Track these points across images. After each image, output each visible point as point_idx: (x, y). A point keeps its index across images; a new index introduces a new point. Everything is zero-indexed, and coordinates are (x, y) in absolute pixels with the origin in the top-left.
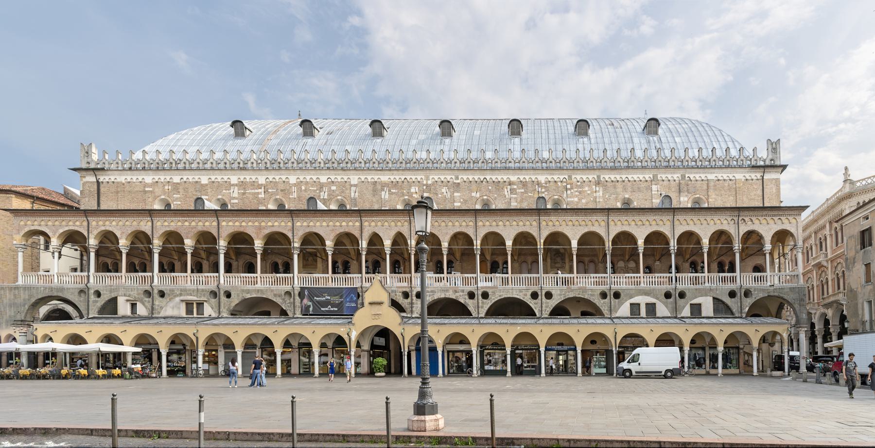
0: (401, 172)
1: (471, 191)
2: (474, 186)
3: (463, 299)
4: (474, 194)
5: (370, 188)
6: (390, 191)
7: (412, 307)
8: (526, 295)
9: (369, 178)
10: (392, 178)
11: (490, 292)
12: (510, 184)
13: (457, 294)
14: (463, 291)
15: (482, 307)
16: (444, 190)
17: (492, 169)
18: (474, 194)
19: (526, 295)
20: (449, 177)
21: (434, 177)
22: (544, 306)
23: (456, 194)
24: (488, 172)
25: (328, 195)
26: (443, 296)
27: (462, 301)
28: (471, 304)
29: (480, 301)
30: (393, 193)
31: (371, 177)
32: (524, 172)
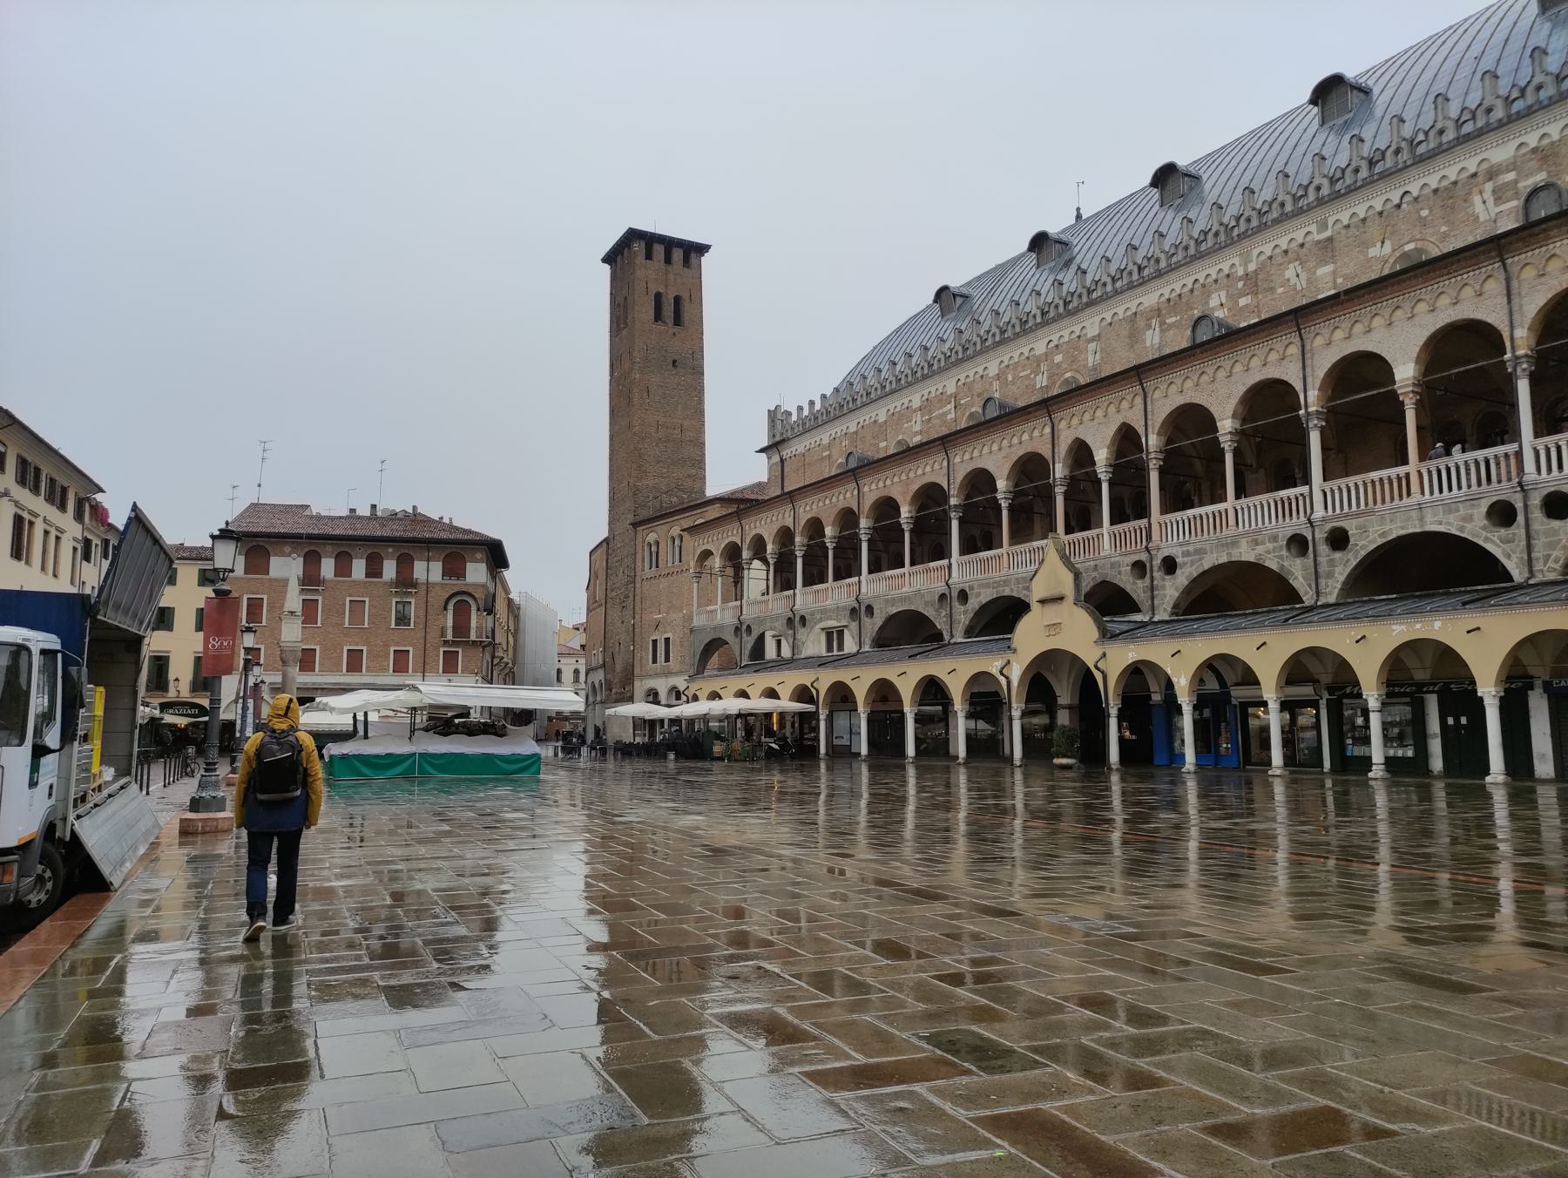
0: (1183, 271)
1: (1367, 245)
2: (1374, 229)
3: (1274, 558)
4: (1374, 252)
5: (1125, 333)
6: (1162, 323)
7: (1153, 598)
8: (1470, 518)
9: (1120, 311)
10: (1166, 291)
11: (1351, 526)
12: (1492, 174)
13: (1260, 549)
14: (1274, 538)
15: (1330, 575)
16: (1290, 273)
17: (1421, 160)
18: (1374, 252)
19: (1470, 518)
20: (1304, 231)
21: (1264, 247)
22: (1539, 544)
23: (1320, 272)
24: (1414, 171)
25: (1049, 378)
26: (1224, 559)
27: (1273, 565)
28: (1298, 573)
29: (1322, 560)
30: (1171, 326)
31: (1123, 307)
32: (1539, 117)
